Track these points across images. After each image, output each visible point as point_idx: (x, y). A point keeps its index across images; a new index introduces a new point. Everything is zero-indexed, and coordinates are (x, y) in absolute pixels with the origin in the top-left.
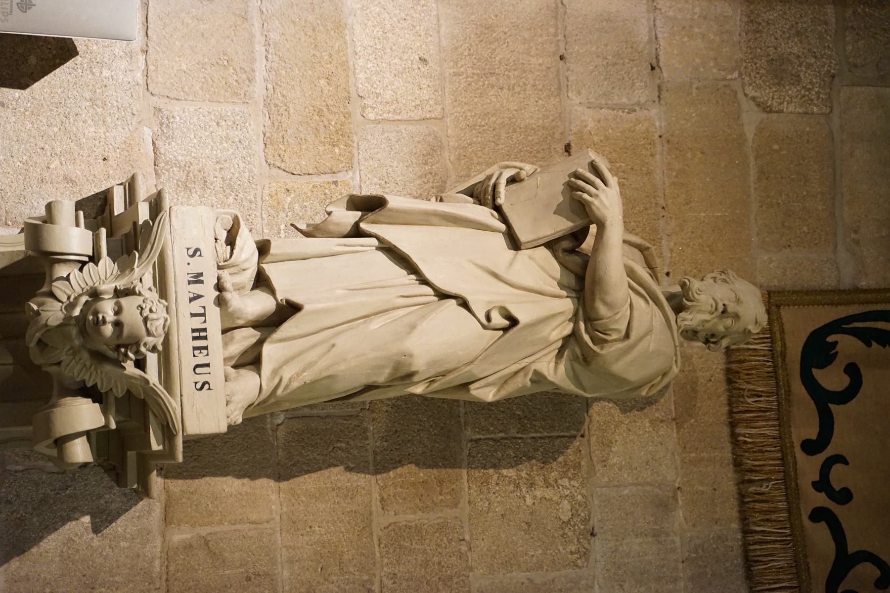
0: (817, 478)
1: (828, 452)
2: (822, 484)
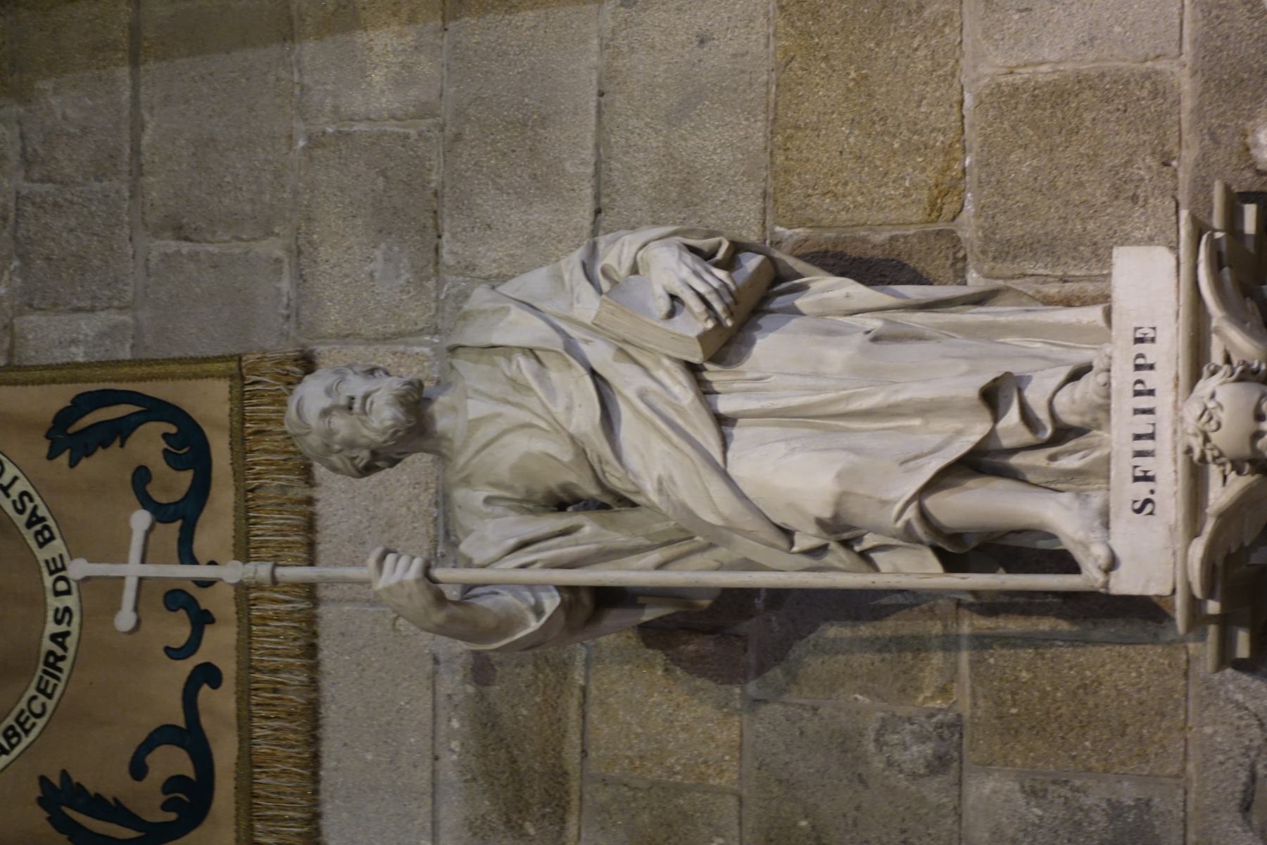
1: (187, 666)
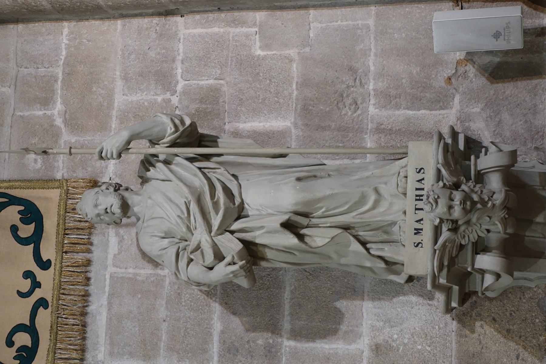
0: (37, 290)
2: (36, 285)
